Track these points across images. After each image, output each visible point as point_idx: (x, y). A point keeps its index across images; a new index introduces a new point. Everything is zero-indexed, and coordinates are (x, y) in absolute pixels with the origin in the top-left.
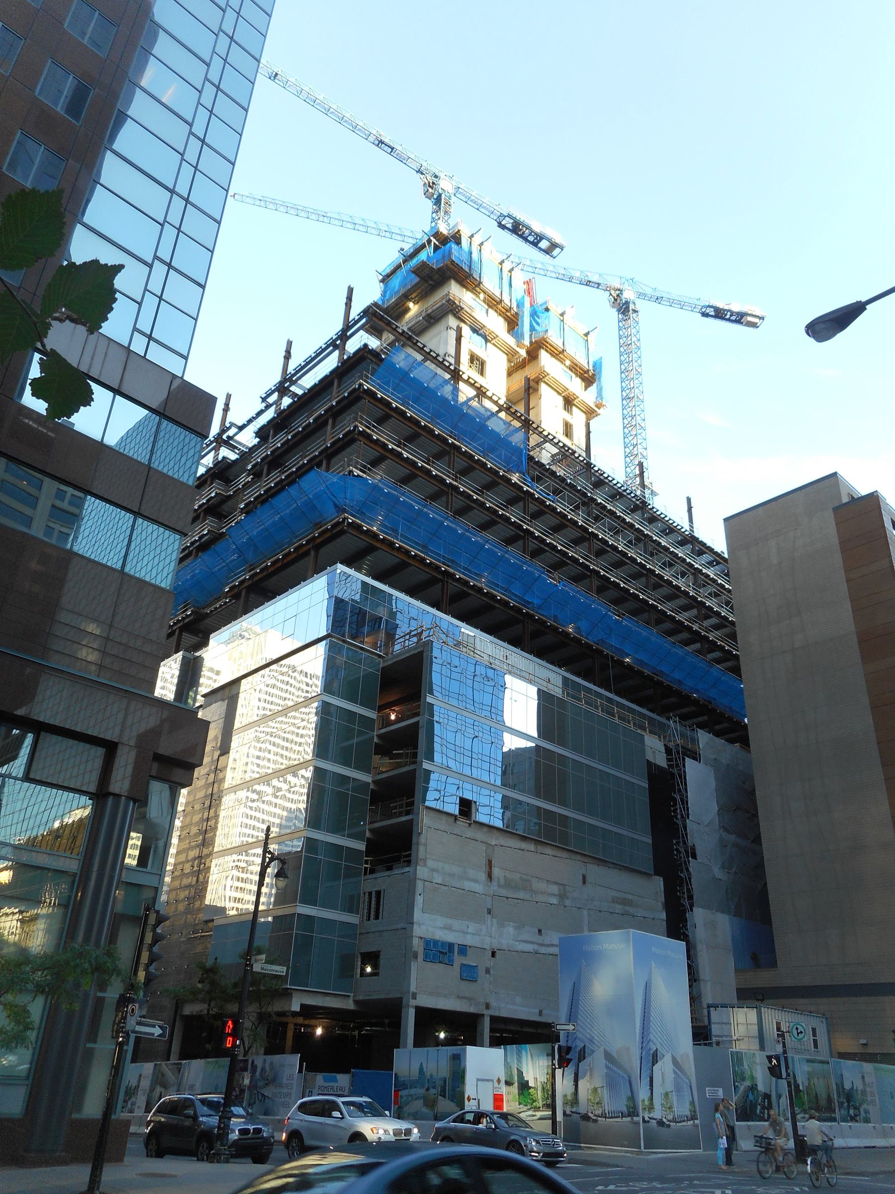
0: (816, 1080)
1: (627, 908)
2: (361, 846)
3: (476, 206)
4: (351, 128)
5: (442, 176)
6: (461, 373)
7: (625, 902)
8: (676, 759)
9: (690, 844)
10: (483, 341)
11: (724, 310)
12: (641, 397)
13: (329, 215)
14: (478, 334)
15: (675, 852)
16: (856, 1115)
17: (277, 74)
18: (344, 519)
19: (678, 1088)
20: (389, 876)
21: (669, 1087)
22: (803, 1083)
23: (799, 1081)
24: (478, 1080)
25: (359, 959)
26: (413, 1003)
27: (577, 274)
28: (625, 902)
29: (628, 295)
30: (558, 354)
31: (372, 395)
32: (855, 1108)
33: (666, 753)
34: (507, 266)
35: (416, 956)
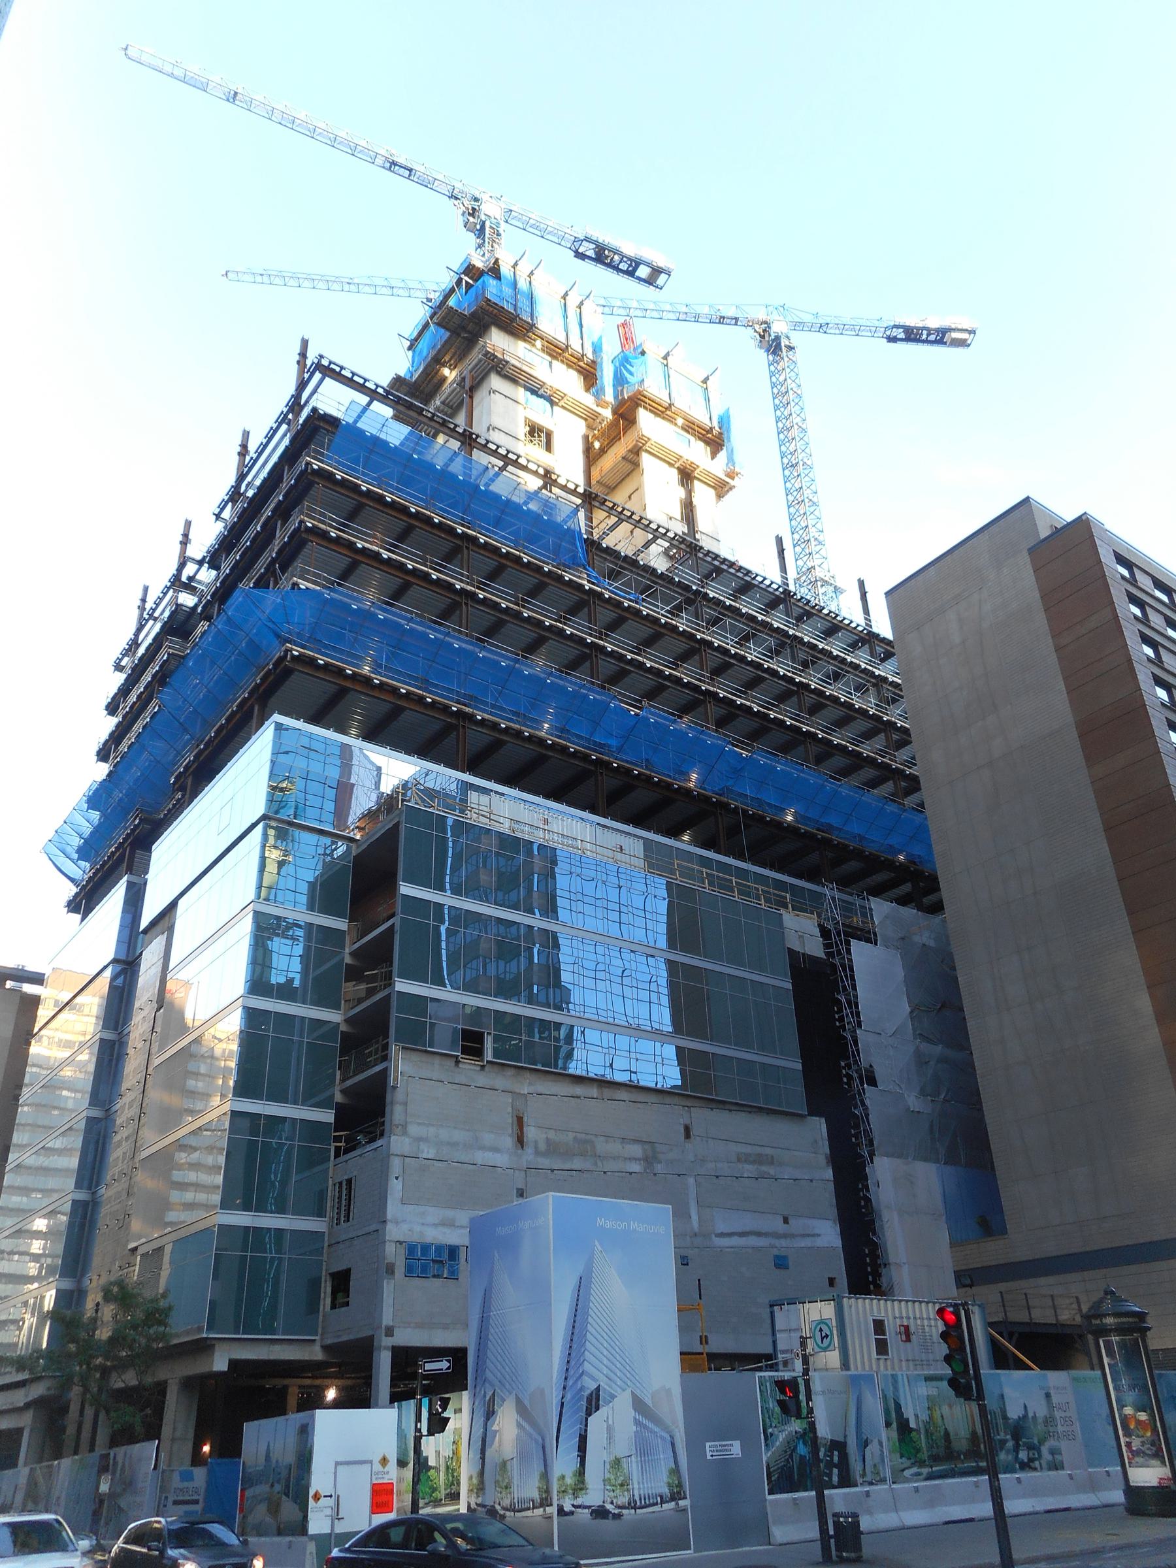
0: (945, 1410)
1: (764, 1168)
2: (327, 1116)
3: (539, 233)
4: (349, 151)
5: (485, 197)
6: (474, 436)
7: (759, 1160)
8: (836, 942)
9: (864, 1064)
10: (548, 405)
11: (918, 329)
12: (809, 463)
13: (356, 281)
14: (538, 396)
15: (845, 1080)
16: (1031, 1460)
17: (236, 93)
18: (287, 651)
19: (644, 1449)
20: (360, 1155)
21: (623, 1447)
22: (916, 1416)
23: (909, 1413)
24: (337, 1464)
25: (329, 1284)
26: (388, 1342)
27: (705, 310)
28: (759, 1160)
29: (777, 328)
30: (663, 411)
31: (329, 476)
32: (1030, 1447)
33: (821, 936)
34: (573, 301)
35: (390, 1269)
